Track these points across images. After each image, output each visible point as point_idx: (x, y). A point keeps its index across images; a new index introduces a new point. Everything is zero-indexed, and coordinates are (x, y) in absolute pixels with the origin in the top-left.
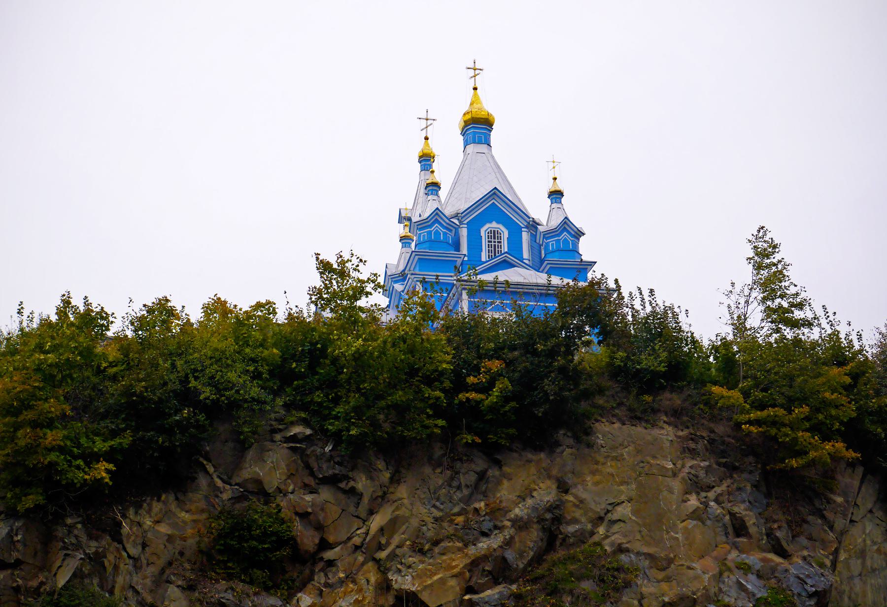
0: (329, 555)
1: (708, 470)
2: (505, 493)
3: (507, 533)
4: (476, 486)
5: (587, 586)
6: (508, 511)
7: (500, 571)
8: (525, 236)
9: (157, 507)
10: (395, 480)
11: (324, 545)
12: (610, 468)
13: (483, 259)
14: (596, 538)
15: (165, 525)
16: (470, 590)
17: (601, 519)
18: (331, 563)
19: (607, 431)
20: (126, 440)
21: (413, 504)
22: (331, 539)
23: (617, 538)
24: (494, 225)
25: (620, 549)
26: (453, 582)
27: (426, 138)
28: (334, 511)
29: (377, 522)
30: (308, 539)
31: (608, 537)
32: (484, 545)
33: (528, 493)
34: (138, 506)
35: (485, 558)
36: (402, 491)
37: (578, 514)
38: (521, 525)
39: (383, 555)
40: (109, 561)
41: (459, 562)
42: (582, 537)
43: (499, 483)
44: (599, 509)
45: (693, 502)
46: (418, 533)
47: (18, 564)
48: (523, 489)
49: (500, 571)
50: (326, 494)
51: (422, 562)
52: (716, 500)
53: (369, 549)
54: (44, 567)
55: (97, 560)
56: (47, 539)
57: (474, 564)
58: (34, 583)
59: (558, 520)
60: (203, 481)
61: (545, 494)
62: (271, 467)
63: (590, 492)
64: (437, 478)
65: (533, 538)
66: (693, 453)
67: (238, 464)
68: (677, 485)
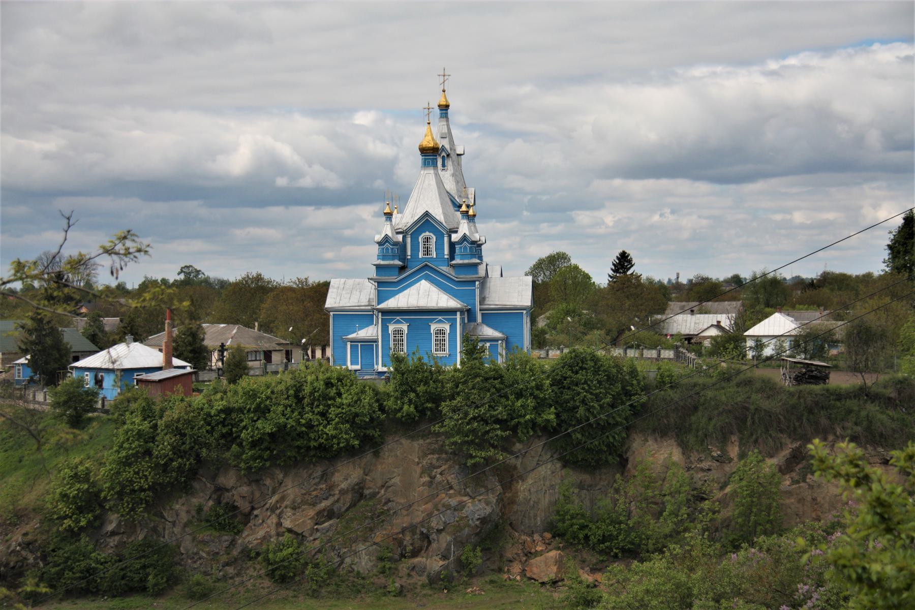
0: (256, 512)
1: (438, 459)
2: (337, 478)
3: (336, 497)
4: (322, 476)
6: (338, 485)
7: (330, 514)
8: (446, 239)
10: (286, 475)
11: (253, 508)
13: (420, 256)
14: (379, 495)
16: (316, 524)
17: (383, 486)
18: (256, 516)
21: (292, 489)
22: (256, 506)
23: (389, 495)
24: (427, 234)
26: (309, 521)
27: (444, 91)
28: (257, 494)
30: (244, 506)
32: (324, 504)
35: (324, 510)
37: (371, 485)
38: (343, 492)
39: (278, 512)
40: (160, 529)
41: (312, 513)
42: (374, 495)
43: (333, 474)
45: (426, 479)
46: (294, 501)
47: (123, 533)
48: (346, 475)
49: (330, 514)
51: (294, 514)
52: (441, 474)
53: (273, 509)
55: (155, 530)
57: (319, 513)
58: (130, 540)
59: (362, 488)
65: (349, 498)
68: (418, 469)
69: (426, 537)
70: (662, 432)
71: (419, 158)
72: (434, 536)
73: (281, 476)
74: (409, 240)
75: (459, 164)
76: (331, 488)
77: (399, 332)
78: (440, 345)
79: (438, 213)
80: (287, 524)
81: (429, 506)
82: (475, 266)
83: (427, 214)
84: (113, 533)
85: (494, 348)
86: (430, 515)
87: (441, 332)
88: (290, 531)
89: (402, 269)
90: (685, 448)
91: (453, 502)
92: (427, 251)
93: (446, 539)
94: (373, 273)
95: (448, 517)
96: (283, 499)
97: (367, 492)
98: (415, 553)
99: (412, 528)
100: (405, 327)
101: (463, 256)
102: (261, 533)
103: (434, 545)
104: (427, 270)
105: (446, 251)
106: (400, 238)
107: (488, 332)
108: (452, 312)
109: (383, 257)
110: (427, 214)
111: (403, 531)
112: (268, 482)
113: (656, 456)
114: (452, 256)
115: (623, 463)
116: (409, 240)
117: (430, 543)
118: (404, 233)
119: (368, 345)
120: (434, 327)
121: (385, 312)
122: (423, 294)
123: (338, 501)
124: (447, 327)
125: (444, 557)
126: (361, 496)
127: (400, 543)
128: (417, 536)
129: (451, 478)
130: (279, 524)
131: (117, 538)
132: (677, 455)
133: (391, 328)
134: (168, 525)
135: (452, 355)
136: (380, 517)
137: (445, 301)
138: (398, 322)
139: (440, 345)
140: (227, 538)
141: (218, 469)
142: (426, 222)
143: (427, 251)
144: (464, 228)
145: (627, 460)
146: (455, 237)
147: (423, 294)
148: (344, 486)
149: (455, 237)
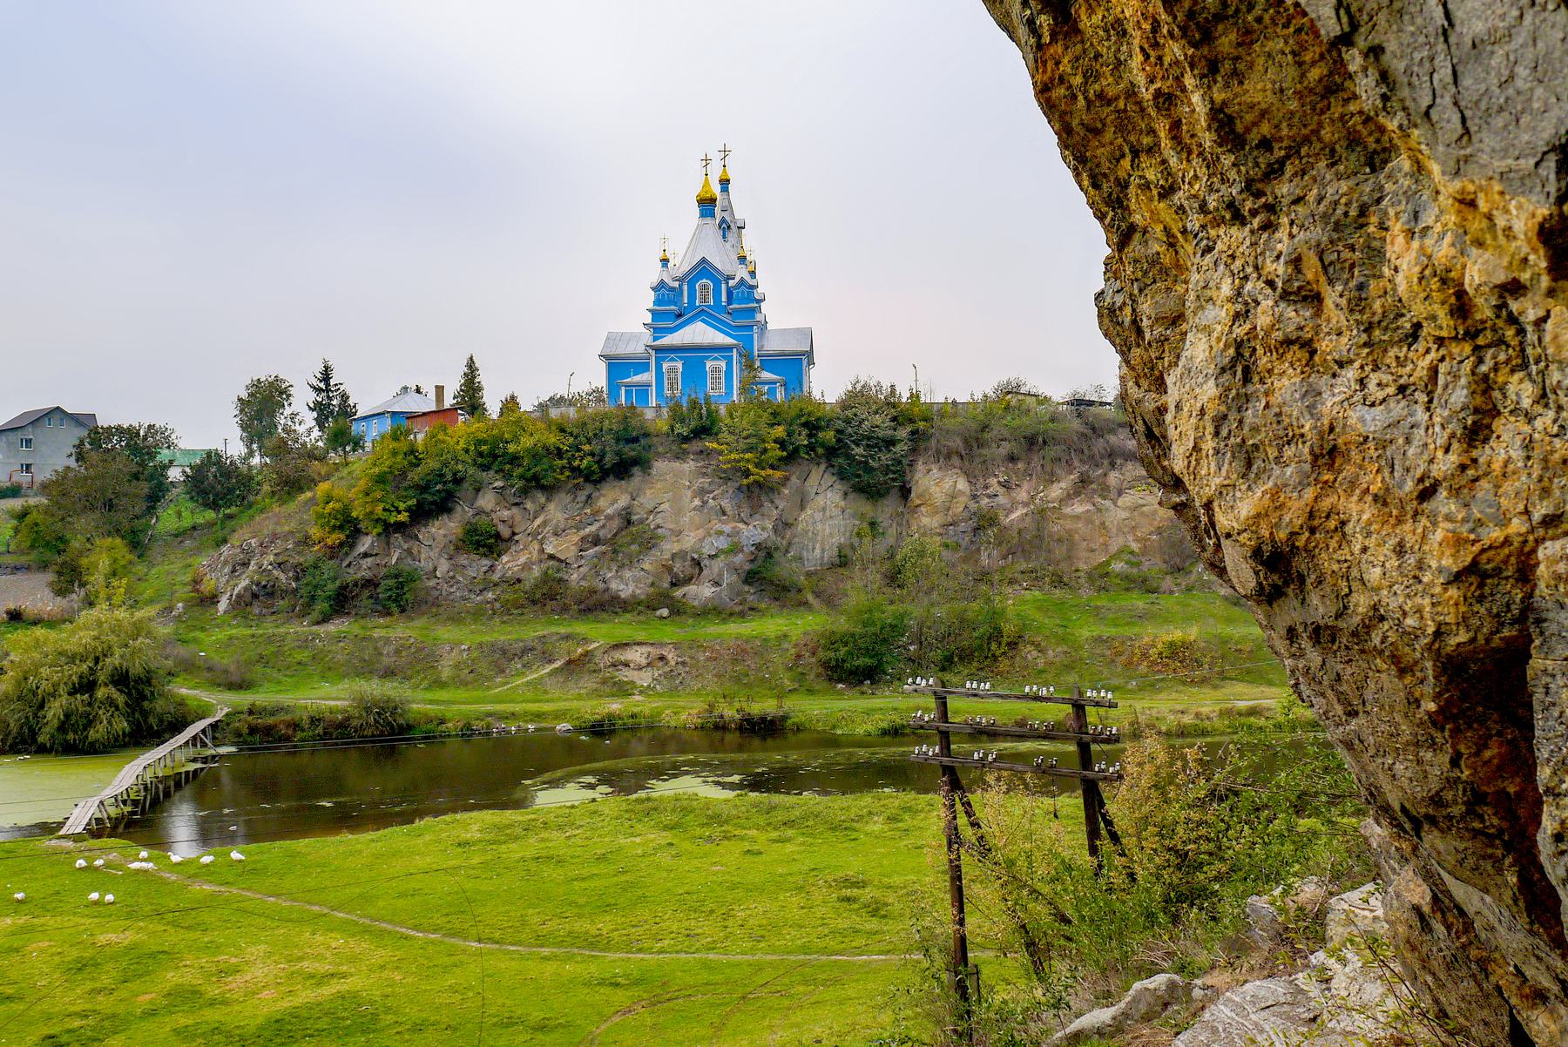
2: (602, 503)
5: (634, 548)
7: (596, 541)
9: (437, 523)
10: (549, 500)
11: (514, 534)
12: (659, 486)
15: (443, 530)
19: (660, 466)
20: (414, 501)
21: (556, 511)
23: (659, 521)
25: (658, 527)
29: (538, 521)
30: (505, 532)
31: (652, 521)
33: (615, 501)
34: (426, 526)
36: (551, 507)
38: (609, 518)
40: (415, 551)
41: (576, 538)
42: (641, 521)
44: (650, 506)
45: (697, 502)
48: (612, 499)
49: (596, 541)
50: (515, 510)
53: (534, 535)
54: (389, 555)
55: (409, 552)
56: (388, 543)
60: (459, 508)
61: (623, 501)
62: (487, 501)
63: (647, 499)
64: (569, 498)
65: (615, 524)
66: (705, 474)
67: (475, 498)
68: (689, 493)
69: (697, 563)
70: (945, 457)
71: (696, 210)
72: (706, 562)
73: (543, 500)
74: (685, 287)
75: (740, 236)
76: (596, 513)
77: (671, 370)
78: (716, 380)
79: (716, 261)
80: (550, 550)
81: (701, 532)
82: (753, 310)
83: (704, 260)
84: (366, 555)
85: (772, 392)
86: (702, 540)
87: (716, 370)
88: (552, 557)
89: (680, 316)
90: (970, 477)
91: (727, 528)
92: (705, 299)
93: (717, 565)
94: (648, 318)
95: (722, 543)
96: (545, 523)
97: (634, 518)
98: (688, 580)
99: (681, 555)
100: (679, 365)
101: (741, 301)
102: (523, 560)
103: (705, 572)
104: (702, 314)
105: (724, 298)
106: (676, 284)
107: (766, 375)
108: (729, 348)
109: (657, 302)
110: (704, 260)
111: (674, 556)
112: (529, 505)
113: (938, 484)
114: (729, 302)
115: (905, 492)
116: (685, 287)
117: (701, 570)
118: (681, 280)
119: (643, 389)
120: (709, 364)
121: (658, 350)
122: (698, 333)
123: (603, 526)
124: (723, 364)
125: (717, 584)
126: (629, 522)
127: (669, 569)
128: (688, 563)
129: (726, 504)
130: (542, 551)
131: (369, 560)
132: (962, 485)
133: (665, 366)
134: (424, 550)
135: (729, 393)
136: (649, 542)
137: (721, 339)
138: (672, 360)
139: (716, 380)
140: (486, 562)
141: (478, 490)
142: (703, 268)
143: (705, 299)
144: (742, 273)
145: (909, 491)
146: (731, 283)
147: (698, 333)
148: (609, 511)
149: (731, 283)
